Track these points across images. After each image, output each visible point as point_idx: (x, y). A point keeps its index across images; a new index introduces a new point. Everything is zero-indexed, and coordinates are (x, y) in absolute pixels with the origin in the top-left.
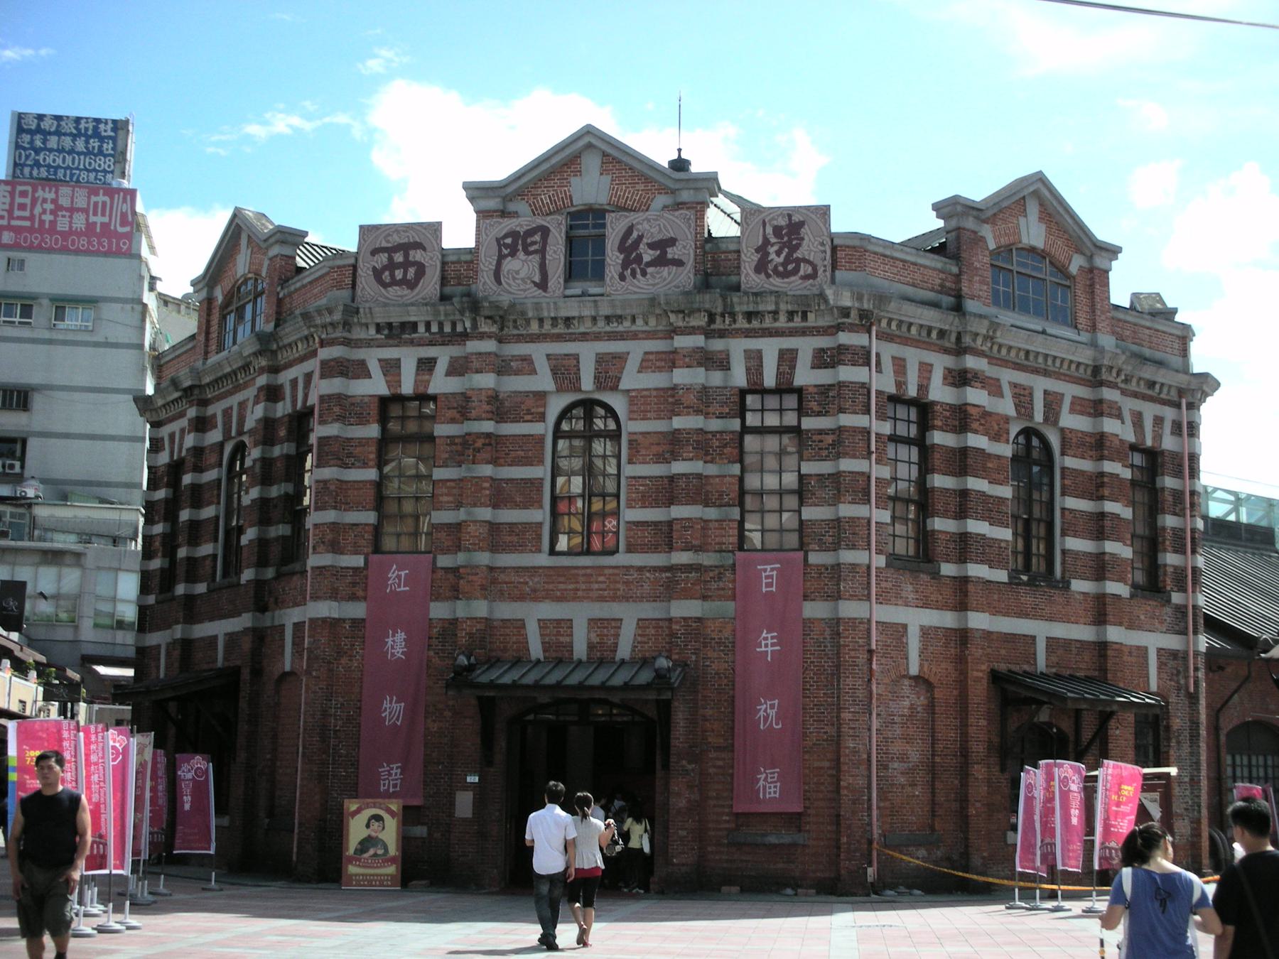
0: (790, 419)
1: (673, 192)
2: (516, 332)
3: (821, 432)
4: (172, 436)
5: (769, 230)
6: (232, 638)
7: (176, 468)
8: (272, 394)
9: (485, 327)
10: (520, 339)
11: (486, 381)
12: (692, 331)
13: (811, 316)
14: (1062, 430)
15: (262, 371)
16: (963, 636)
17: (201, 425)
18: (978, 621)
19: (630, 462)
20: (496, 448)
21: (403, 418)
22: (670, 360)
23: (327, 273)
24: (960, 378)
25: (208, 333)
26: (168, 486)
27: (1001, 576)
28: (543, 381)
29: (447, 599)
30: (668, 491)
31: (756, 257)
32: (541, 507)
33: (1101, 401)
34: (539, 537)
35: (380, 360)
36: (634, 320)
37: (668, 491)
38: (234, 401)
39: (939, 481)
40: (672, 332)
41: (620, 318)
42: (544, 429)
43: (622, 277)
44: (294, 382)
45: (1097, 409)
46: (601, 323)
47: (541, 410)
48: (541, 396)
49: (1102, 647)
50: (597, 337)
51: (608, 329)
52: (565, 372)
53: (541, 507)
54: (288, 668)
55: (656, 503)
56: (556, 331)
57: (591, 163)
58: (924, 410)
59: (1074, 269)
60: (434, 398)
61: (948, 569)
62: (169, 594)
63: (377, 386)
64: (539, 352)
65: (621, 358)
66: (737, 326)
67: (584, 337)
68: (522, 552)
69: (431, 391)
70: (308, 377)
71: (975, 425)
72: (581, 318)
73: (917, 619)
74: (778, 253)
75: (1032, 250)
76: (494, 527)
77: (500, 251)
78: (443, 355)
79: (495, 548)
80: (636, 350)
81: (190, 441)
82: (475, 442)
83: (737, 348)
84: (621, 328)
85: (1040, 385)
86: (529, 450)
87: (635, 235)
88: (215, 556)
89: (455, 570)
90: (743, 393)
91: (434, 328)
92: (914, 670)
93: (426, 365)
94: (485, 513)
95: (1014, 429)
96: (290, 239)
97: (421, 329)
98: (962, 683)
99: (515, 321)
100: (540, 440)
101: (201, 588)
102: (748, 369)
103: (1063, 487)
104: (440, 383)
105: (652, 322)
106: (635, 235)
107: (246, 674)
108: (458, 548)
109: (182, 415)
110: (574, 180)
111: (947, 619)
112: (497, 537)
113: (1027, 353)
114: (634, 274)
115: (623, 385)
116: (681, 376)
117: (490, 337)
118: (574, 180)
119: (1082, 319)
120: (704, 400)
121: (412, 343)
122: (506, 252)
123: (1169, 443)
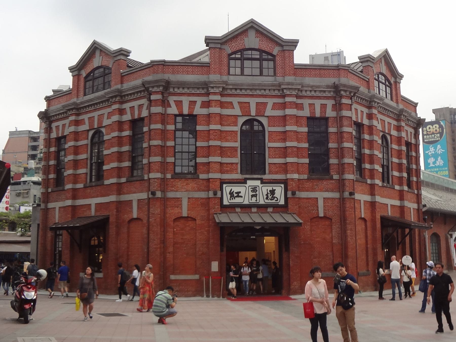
0: (323, 129)
1: (282, 46)
4: (57, 127)
6: (99, 206)
7: (60, 140)
8: (121, 112)
14: (391, 135)
15: (115, 103)
16: (373, 204)
17: (77, 123)
18: (378, 199)
19: (269, 142)
20: (221, 135)
22: (284, 106)
23: (152, 67)
24: (370, 117)
25: (78, 88)
26: (55, 146)
27: (380, 185)
28: (237, 111)
29: (203, 191)
30: (284, 152)
32: (237, 157)
33: (401, 126)
37: (284, 152)
38: (96, 114)
39: (367, 151)
42: (237, 129)
44: (132, 108)
45: (399, 128)
48: (236, 117)
49: (402, 209)
54: (135, 216)
55: (280, 157)
57: (252, 34)
59: (392, 82)
60: (196, 116)
61: (369, 181)
62: (61, 188)
64: (235, 101)
65: (265, 104)
67: (252, 96)
68: (231, 173)
69: (194, 113)
70: (141, 106)
71: (374, 132)
75: (382, 74)
76: (221, 164)
78: (199, 100)
79: (222, 172)
80: (270, 102)
81: (72, 129)
83: (306, 102)
85: (387, 120)
88: (86, 173)
89: (208, 180)
90: (308, 118)
92: (363, 216)
93: (192, 103)
94: (218, 159)
95: (381, 134)
96: (125, 53)
98: (373, 220)
101: (80, 186)
103: (391, 154)
104: (198, 110)
105: (276, 92)
107: (112, 219)
108: (208, 172)
109: (67, 118)
110: (245, 39)
111: (368, 198)
112: (222, 168)
113: (385, 109)
116: (288, 111)
117: (218, 95)
118: (245, 39)
119: (394, 98)
120: (297, 120)
123: (413, 141)
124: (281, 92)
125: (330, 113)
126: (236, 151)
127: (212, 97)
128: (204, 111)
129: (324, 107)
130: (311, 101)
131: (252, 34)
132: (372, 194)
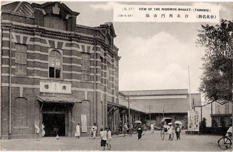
10: (44, 36)
11: (39, 43)
16: (105, 95)
22: (71, 45)
24: (105, 54)
28: (48, 45)
33: (113, 60)
40: (71, 40)
52: (52, 43)
57: (56, 6)
58: (101, 58)
64: (47, 40)
73: (102, 92)
78: (29, 37)
80: (65, 42)
83: (80, 44)
104: (28, 42)
125: (91, 51)
127: (36, 36)
128: (32, 43)
129: (89, 48)
130: (83, 44)
131: (56, 6)
132: (105, 91)
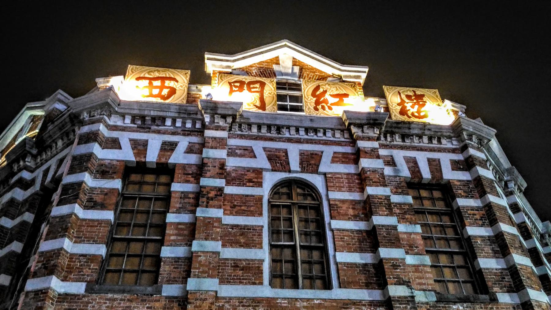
2: (239, 133)
3: (472, 209)
5: (403, 96)
9: (221, 123)
12: (369, 139)
13: (444, 141)
21: (141, 184)
22: (356, 157)
28: (262, 162)
31: (399, 108)
34: (261, 272)
35: (131, 140)
36: (325, 134)
41: (316, 131)
43: (316, 109)
46: (302, 132)
47: (259, 180)
48: (259, 172)
50: (299, 141)
51: (306, 137)
53: (261, 248)
55: (361, 250)
56: (269, 135)
63: (127, 154)
64: (258, 146)
66: (395, 143)
69: (171, 161)
72: (288, 127)
74: (412, 107)
77: (231, 88)
82: (208, 193)
84: (315, 137)
86: (248, 206)
87: (321, 90)
91: (179, 124)
97: (169, 122)
99: (240, 126)
100: (260, 198)
102: (409, 168)
104: (179, 157)
105: (338, 134)
106: (321, 90)
114: (323, 108)
115: (322, 169)
117: (224, 130)
121: (159, 132)
122: (234, 89)
124: (346, 135)
126: (260, 235)
